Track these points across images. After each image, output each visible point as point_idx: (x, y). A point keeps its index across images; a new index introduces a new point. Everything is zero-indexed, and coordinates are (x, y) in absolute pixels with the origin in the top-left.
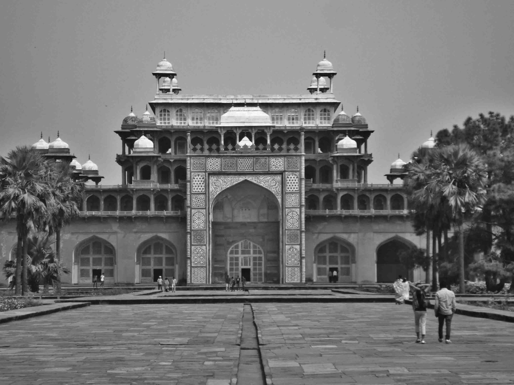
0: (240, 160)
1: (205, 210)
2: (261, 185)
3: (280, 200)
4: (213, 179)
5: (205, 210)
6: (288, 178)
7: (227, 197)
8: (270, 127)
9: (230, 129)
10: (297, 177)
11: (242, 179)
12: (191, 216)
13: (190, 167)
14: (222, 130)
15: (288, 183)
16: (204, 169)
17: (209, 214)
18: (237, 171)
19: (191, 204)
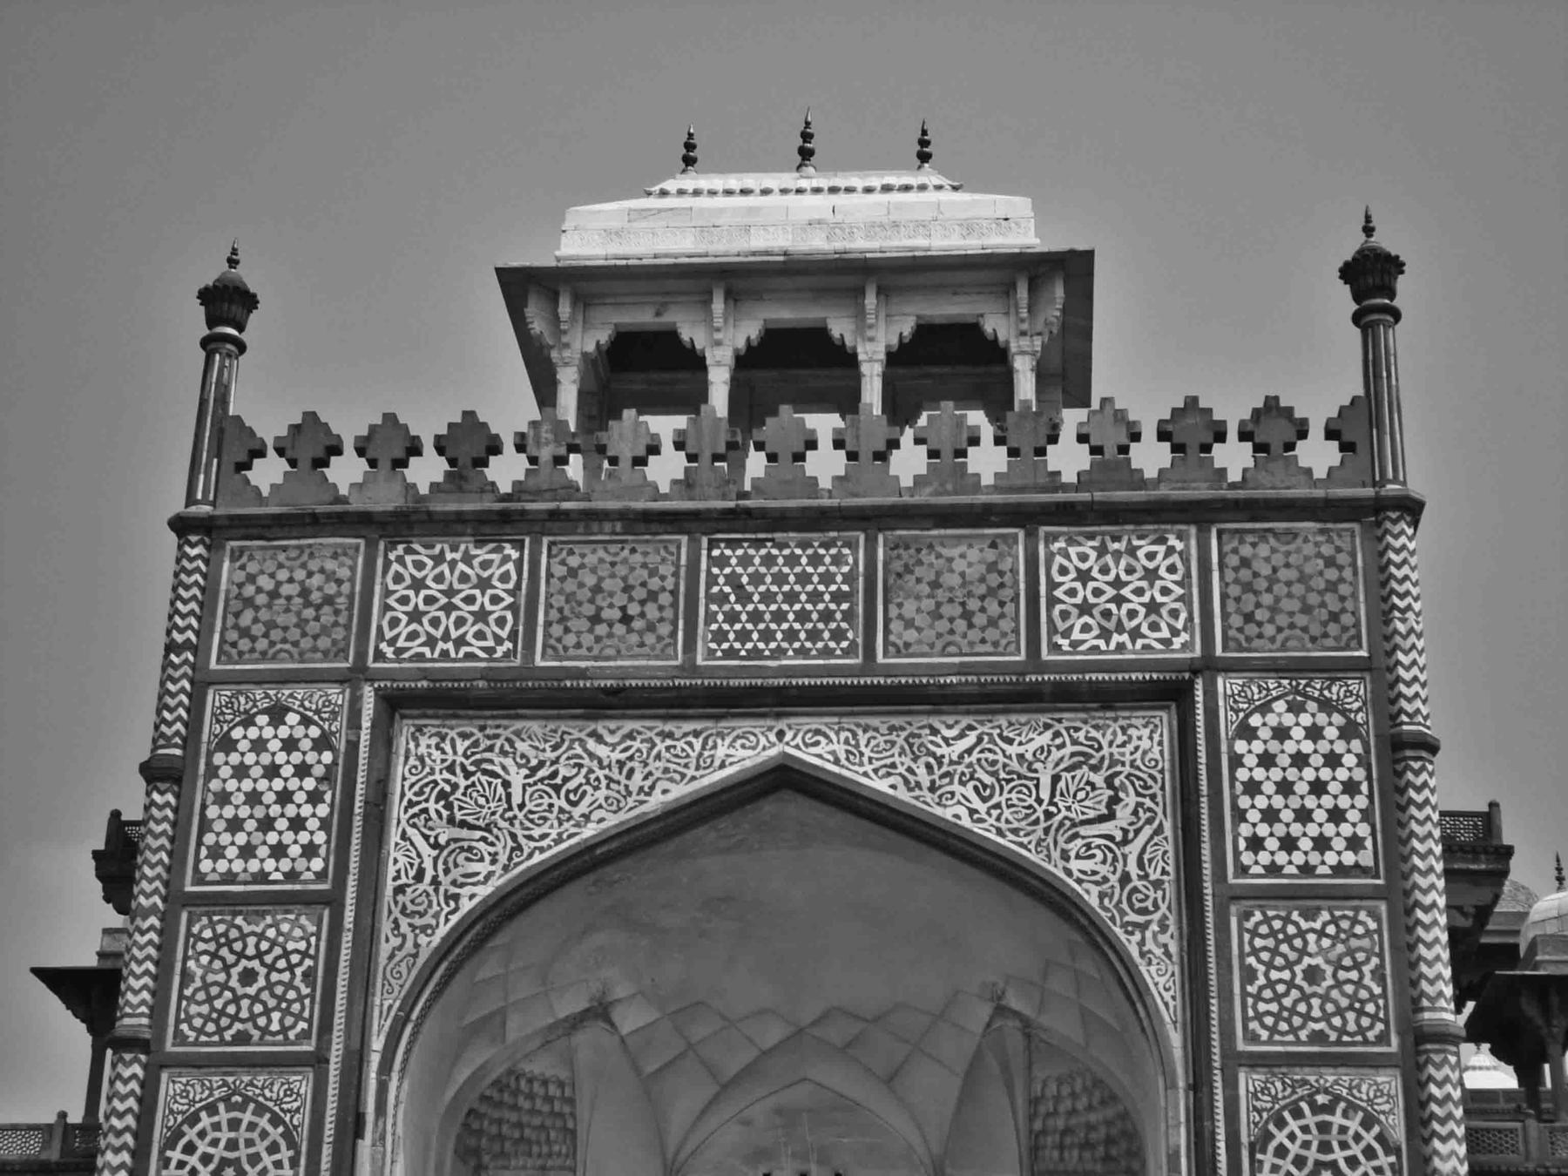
0: (738, 559)
1: (303, 1084)
2: (948, 814)
3: (1162, 980)
4: (427, 753)
5: (303, 1084)
6: (1248, 733)
7: (600, 1011)
9: (642, 317)
10: (1348, 732)
11: (741, 749)
12: (140, 1154)
13: (204, 633)
14: (565, 309)
15: (1253, 788)
16: (342, 652)
17: (352, 1126)
18: (690, 668)
19: (158, 1011)
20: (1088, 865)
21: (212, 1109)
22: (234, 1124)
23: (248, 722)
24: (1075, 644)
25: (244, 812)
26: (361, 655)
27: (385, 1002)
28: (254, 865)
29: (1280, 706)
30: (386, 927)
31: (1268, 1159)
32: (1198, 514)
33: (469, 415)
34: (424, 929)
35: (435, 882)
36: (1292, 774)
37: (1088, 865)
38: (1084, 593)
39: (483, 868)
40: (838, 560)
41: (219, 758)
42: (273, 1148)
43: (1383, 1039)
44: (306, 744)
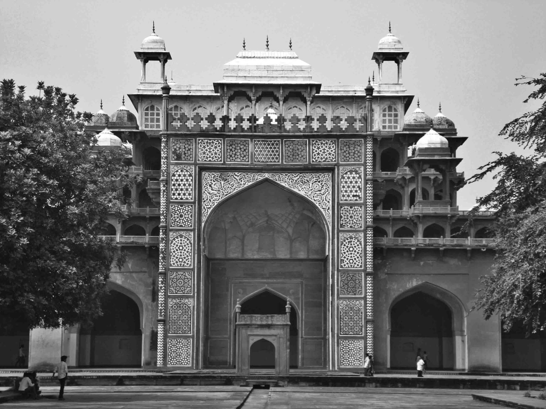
5: (192, 234)
6: (344, 178)
8: (311, 86)
10: (360, 177)
11: (259, 177)
14: (225, 90)
20: (317, 198)
21: (177, 238)
22: (181, 240)
23: (177, 171)
24: (316, 160)
25: (178, 187)
26: (195, 160)
27: (204, 219)
28: (180, 197)
29: (349, 173)
30: (203, 207)
31: (343, 246)
32: (338, 137)
33: (211, 114)
34: (209, 208)
35: (210, 200)
36: (350, 185)
37: (317, 198)
38: (318, 151)
39: (218, 198)
40: (277, 144)
41: (173, 178)
42: (188, 244)
43: (361, 227)
44: (187, 175)
